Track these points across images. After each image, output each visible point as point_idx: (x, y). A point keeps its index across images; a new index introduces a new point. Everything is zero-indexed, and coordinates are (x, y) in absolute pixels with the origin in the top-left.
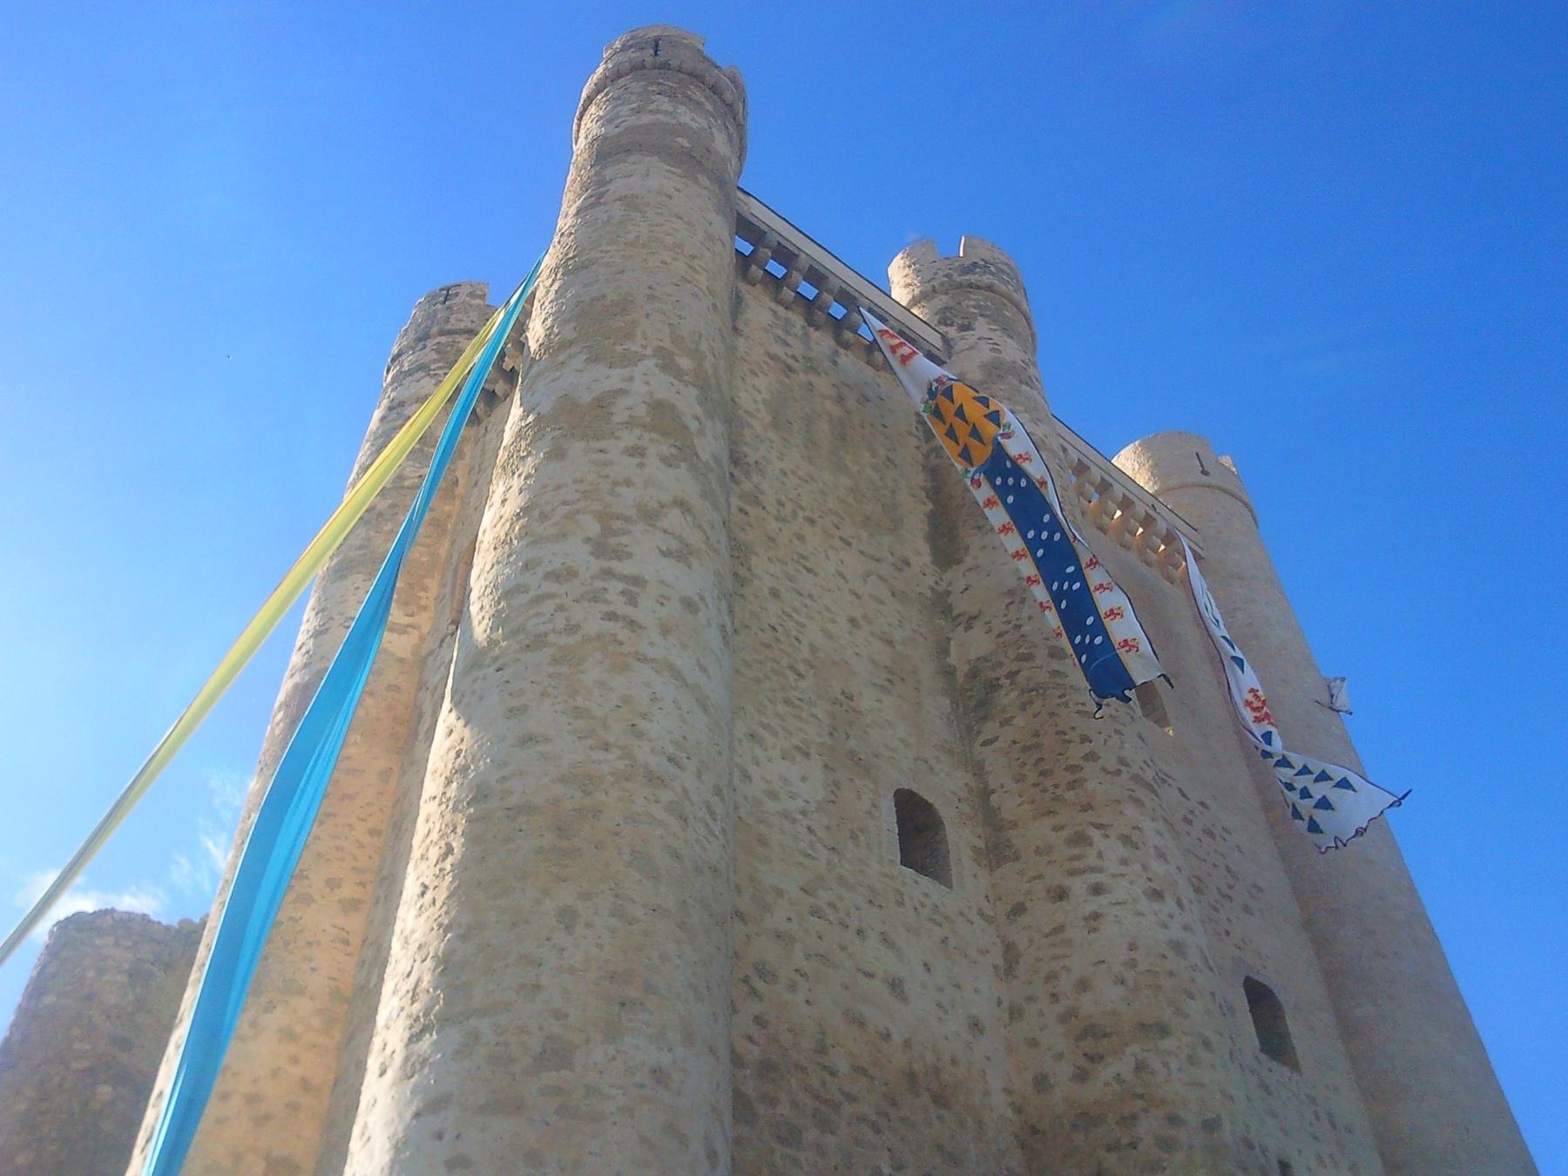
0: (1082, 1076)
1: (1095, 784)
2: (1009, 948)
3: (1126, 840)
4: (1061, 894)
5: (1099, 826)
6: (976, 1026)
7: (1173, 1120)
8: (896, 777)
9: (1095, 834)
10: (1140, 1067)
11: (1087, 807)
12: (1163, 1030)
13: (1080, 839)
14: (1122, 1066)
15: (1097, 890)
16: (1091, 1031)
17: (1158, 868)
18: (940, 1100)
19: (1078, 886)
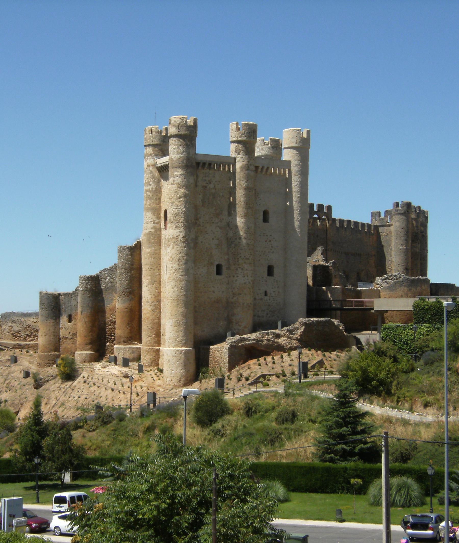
0: (232, 298)
1: (241, 261)
2: (229, 281)
3: (242, 269)
4: (234, 276)
5: (239, 268)
6: (223, 292)
7: (239, 304)
8: (217, 263)
9: (239, 269)
10: (238, 299)
11: (238, 265)
12: (241, 294)
13: (237, 269)
14: (235, 298)
15: (237, 277)
16: (234, 294)
17: (245, 272)
18: (218, 302)
19: (236, 276)
